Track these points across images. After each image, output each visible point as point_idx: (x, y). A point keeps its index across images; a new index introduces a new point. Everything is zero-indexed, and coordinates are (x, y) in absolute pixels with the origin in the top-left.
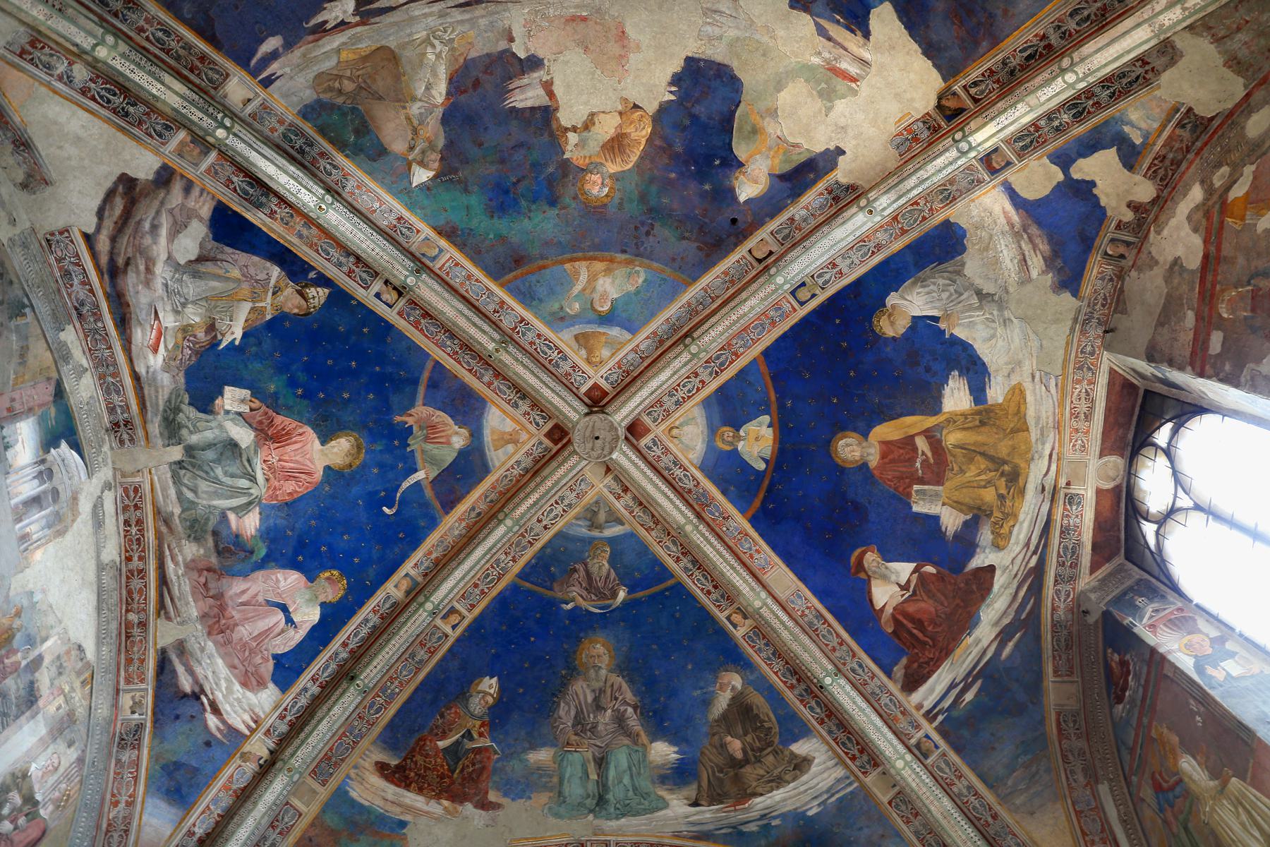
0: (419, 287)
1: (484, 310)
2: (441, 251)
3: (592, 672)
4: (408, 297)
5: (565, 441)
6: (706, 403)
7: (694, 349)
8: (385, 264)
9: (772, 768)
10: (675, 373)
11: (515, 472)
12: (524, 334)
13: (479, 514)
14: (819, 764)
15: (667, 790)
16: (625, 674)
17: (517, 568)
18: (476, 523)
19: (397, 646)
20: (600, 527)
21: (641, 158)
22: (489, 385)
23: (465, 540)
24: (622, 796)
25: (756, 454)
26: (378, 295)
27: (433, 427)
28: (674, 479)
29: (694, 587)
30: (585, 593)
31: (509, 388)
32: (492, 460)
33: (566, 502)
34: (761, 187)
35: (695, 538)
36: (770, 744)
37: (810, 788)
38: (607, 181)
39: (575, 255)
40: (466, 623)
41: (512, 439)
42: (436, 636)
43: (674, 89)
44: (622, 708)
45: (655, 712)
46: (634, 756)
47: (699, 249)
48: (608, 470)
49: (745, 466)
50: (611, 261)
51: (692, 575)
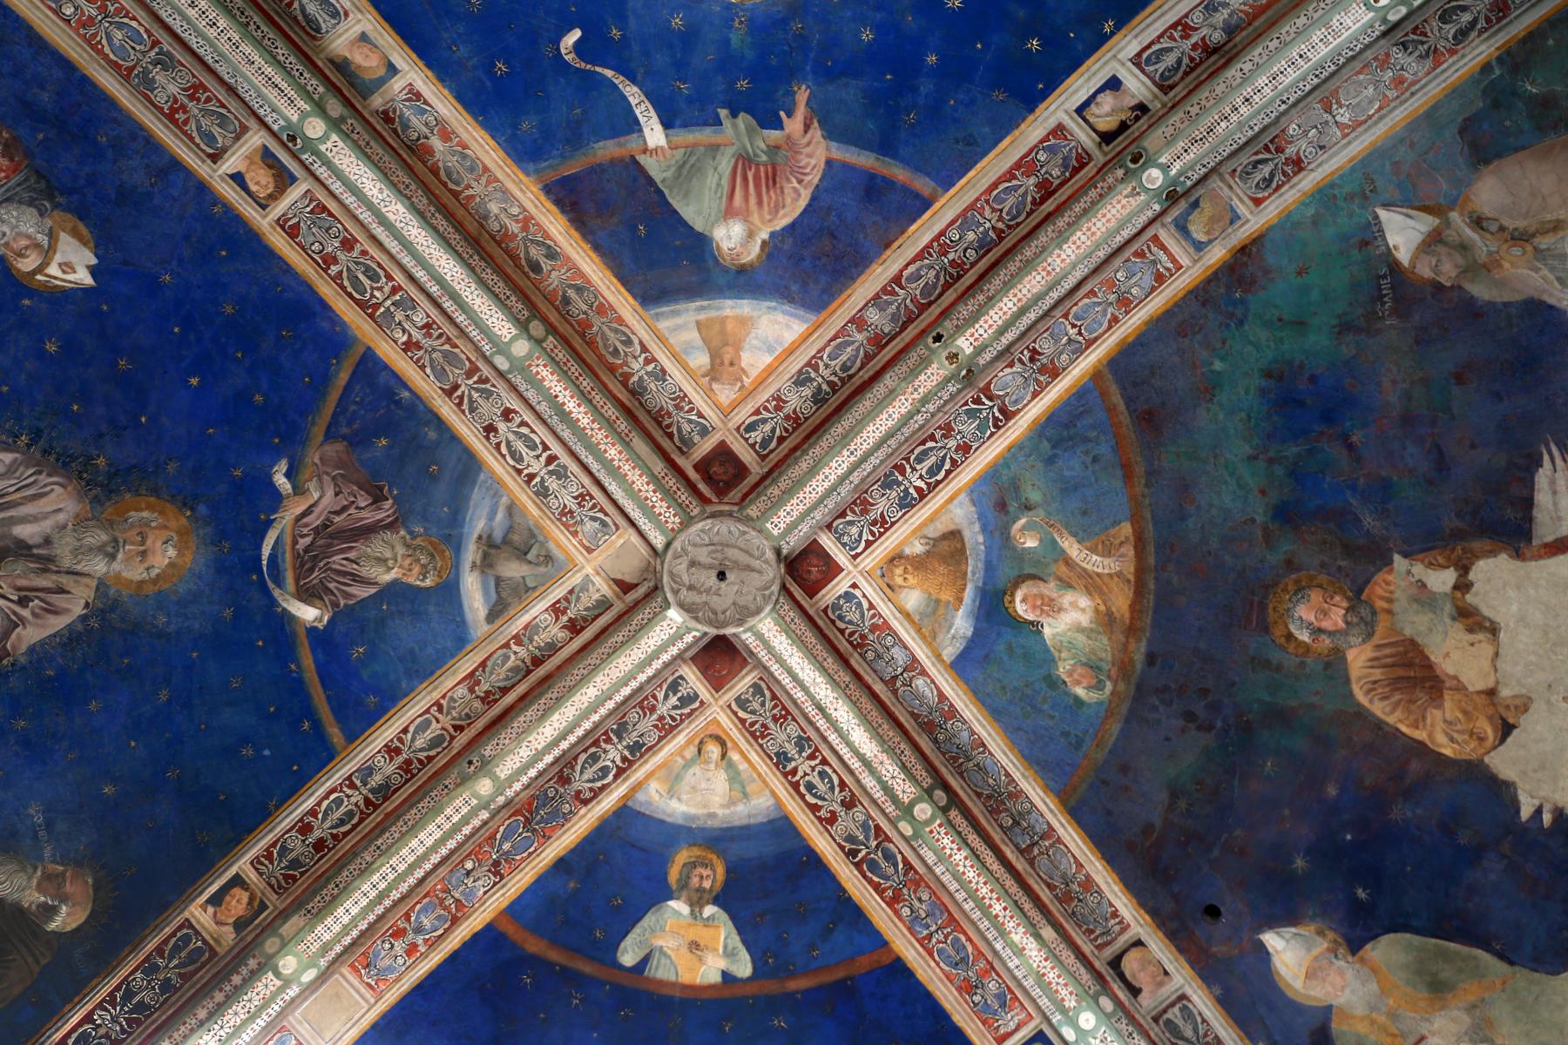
0: (1134, 193)
1: (1041, 327)
2: (1199, 247)
3: (99, 537)
4: (1096, 153)
5: (702, 487)
6: (782, 826)
7: (923, 810)
8: (1207, 121)
10: (866, 763)
11: (636, 366)
12: (971, 414)
13: (536, 268)
17: (389, 352)
18: (515, 258)
19: (212, 33)
20: (486, 564)
21: (1379, 725)
22: (858, 321)
23: (472, 227)
25: (659, 943)
26: (1113, 84)
27: (773, 179)
28: (596, 743)
29: (321, 792)
30: (315, 520)
31: (844, 368)
32: (676, 313)
33: (552, 484)
34: (1298, 984)
35: (458, 802)
38: (1326, 642)
39: (1151, 549)
40: (249, 211)
41: (721, 366)
42: (216, 130)
43: (1547, 818)
47: (1148, 829)
48: (625, 587)
49: (629, 918)
50: (1131, 630)
51: (352, 786)
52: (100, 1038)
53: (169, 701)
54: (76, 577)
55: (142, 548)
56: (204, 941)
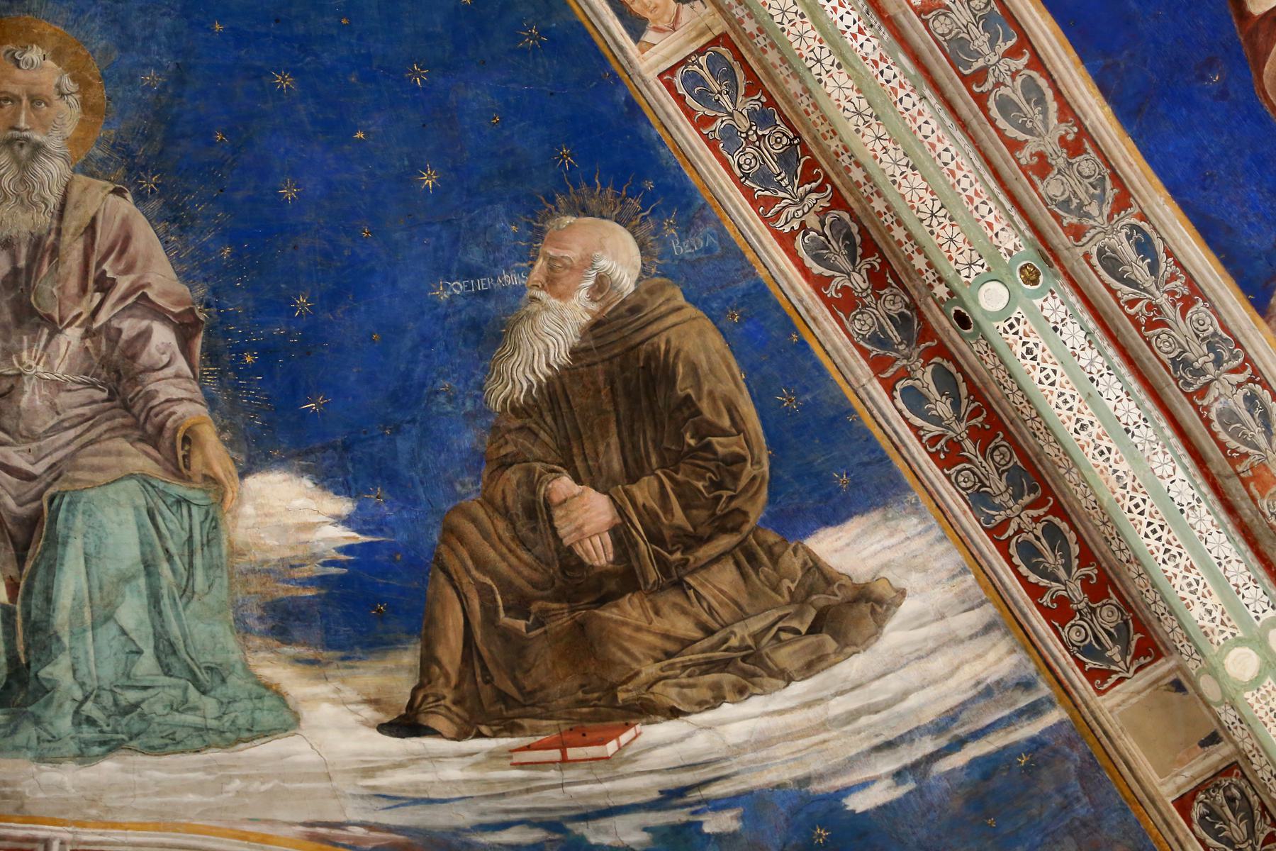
9: (725, 614)
14: (919, 621)
15: (297, 660)
16: (150, 182)
24: (108, 672)
36: (728, 522)
37: (873, 709)
44: (129, 327)
45: (268, 352)
46: (171, 522)
52: (823, 225)
53: (294, 73)
54: (69, 207)
55: (25, 101)
56: (701, 51)
